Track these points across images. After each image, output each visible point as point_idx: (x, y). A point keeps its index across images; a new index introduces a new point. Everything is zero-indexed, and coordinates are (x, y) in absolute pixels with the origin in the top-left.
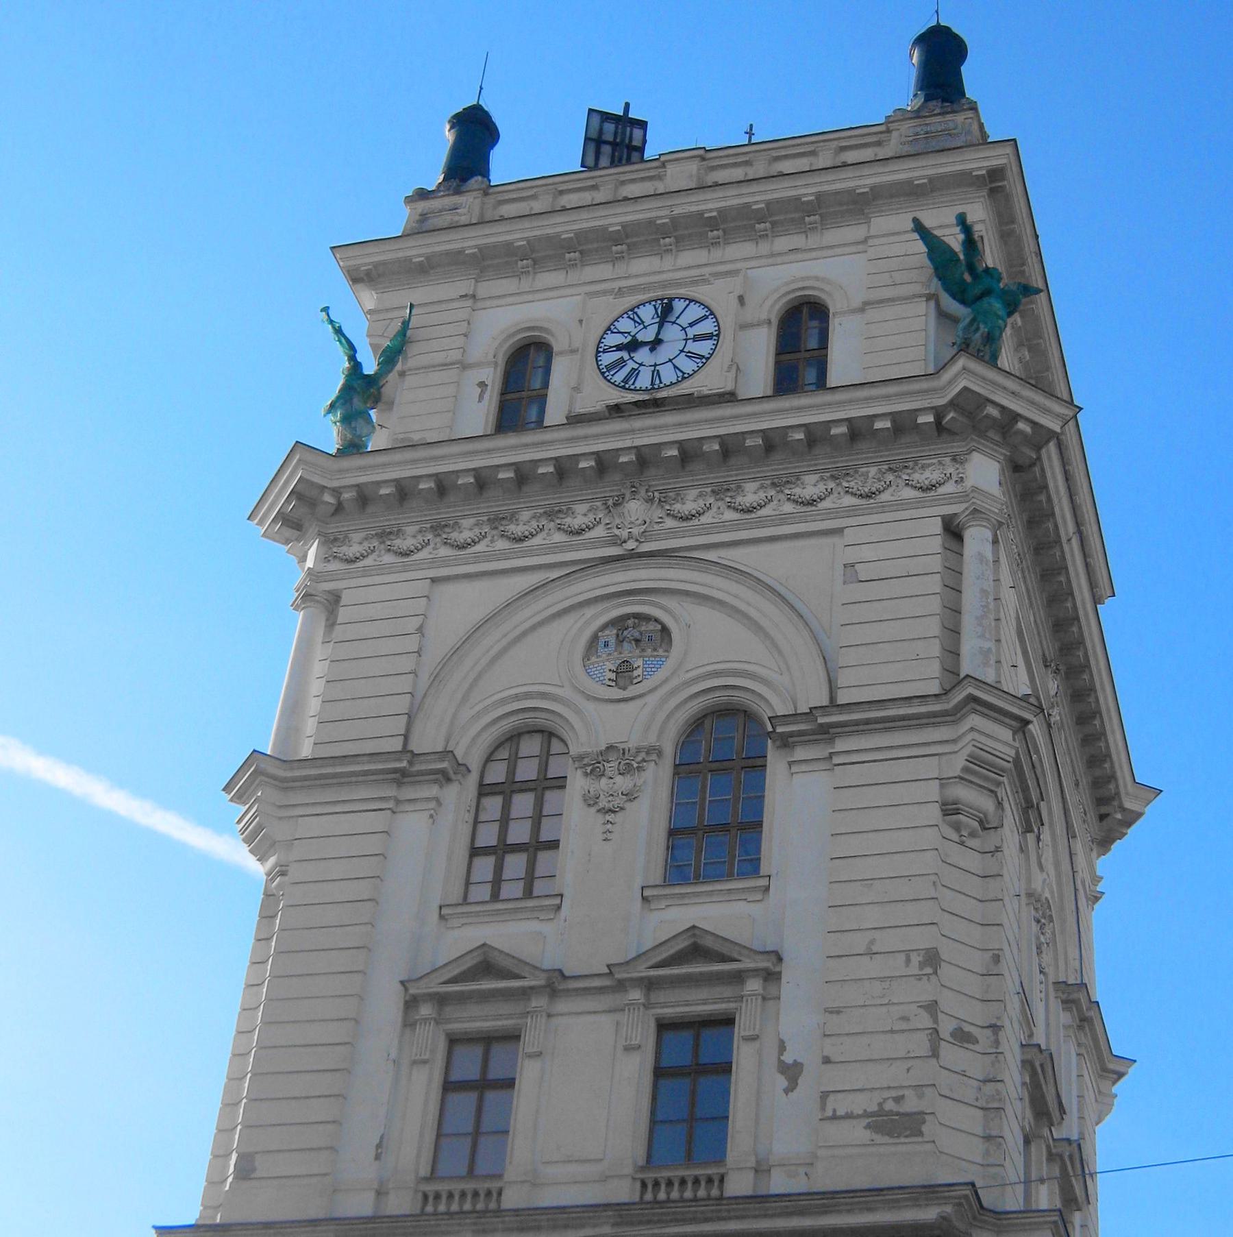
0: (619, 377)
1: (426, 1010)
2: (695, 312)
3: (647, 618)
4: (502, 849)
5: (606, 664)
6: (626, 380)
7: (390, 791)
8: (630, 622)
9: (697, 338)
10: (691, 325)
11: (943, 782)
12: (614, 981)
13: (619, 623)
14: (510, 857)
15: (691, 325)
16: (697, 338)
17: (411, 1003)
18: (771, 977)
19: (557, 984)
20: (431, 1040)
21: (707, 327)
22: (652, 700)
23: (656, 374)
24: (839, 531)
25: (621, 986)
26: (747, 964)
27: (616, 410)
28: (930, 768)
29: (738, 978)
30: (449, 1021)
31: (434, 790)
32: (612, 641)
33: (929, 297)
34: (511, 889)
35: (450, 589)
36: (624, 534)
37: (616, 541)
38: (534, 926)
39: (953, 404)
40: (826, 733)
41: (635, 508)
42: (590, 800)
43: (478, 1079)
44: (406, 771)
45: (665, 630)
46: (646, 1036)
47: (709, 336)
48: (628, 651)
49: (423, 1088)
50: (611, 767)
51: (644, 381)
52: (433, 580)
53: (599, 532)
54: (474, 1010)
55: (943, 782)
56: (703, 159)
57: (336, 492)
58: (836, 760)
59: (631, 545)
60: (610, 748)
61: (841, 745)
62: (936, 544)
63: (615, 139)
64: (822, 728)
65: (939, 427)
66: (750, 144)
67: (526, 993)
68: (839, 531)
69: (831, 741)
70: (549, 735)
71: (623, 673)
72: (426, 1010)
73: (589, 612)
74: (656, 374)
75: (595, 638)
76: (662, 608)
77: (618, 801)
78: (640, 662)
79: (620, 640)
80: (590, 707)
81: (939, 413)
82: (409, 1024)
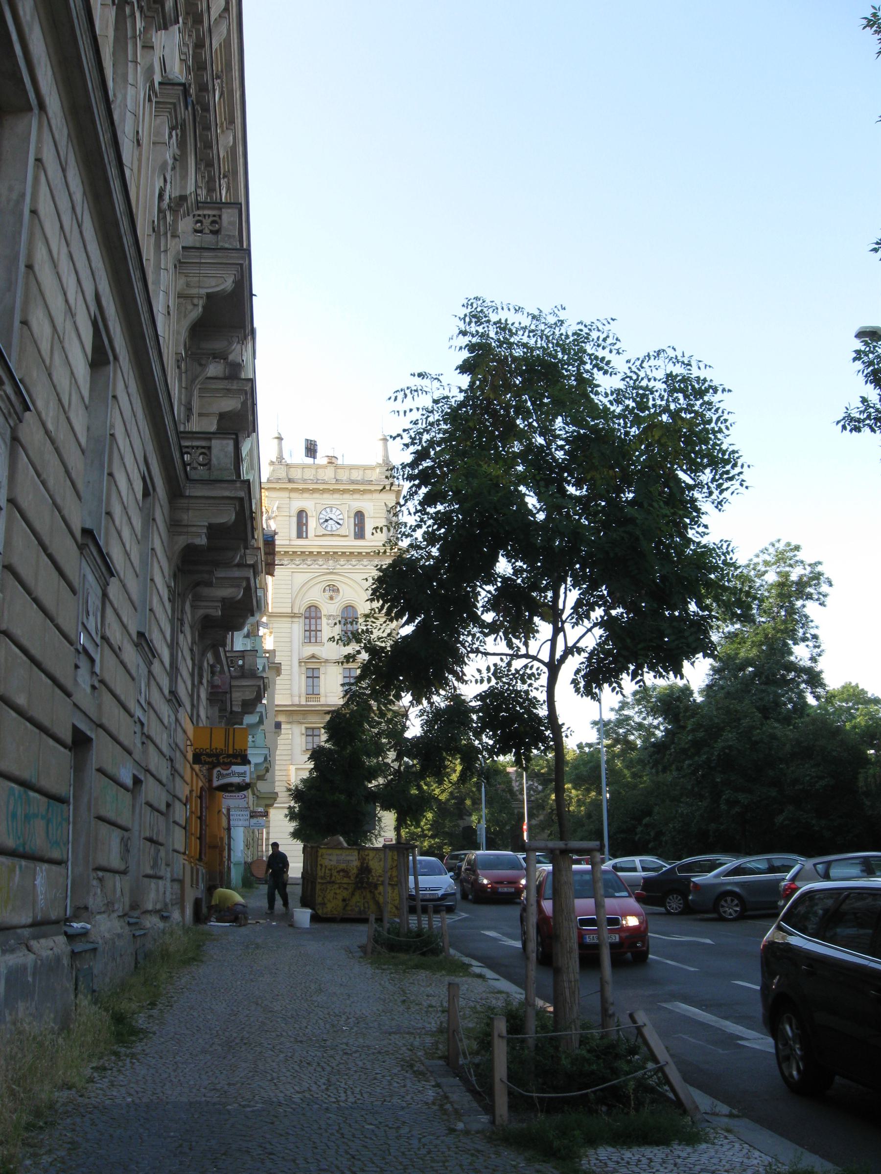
2: (338, 512)
4: (310, 631)
5: (328, 594)
14: (312, 634)
20: (304, 669)
21: (341, 517)
27: (324, 535)
34: (313, 640)
41: (331, 562)
44: (293, 616)
49: (303, 677)
51: (329, 528)
63: (311, 449)
70: (316, 607)
71: (331, 598)
82: (300, 666)
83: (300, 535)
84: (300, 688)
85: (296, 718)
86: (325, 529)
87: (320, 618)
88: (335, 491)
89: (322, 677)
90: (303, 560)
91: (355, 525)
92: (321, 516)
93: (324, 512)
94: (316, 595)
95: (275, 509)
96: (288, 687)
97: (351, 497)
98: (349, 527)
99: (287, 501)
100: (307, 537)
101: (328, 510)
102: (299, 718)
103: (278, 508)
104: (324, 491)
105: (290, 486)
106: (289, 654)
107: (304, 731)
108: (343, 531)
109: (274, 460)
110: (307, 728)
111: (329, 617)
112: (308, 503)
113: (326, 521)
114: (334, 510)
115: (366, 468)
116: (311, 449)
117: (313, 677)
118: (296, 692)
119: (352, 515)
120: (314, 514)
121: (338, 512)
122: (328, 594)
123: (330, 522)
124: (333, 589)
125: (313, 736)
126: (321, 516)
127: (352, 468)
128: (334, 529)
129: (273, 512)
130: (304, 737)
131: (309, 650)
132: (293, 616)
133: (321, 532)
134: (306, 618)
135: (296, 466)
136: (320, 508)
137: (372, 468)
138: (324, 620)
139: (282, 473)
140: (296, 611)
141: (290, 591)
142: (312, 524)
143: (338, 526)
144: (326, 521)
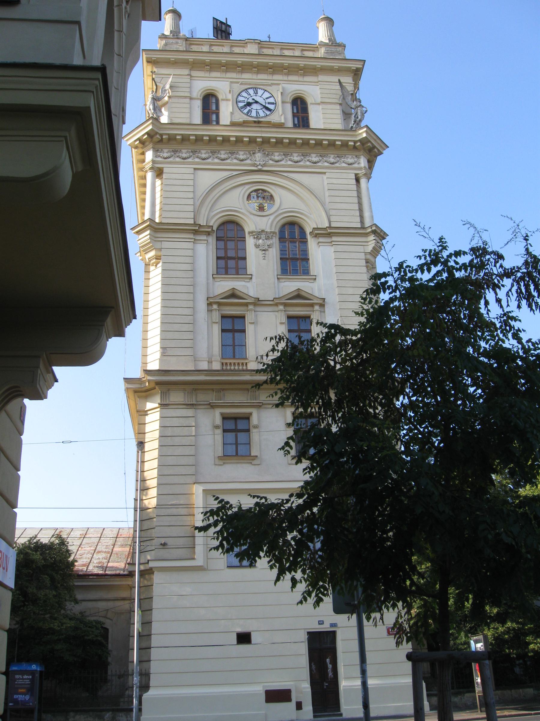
0: (246, 111)
1: (215, 307)
2: (267, 95)
3: (264, 191)
5: (254, 204)
6: (248, 112)
7: (192, 236)
8: (260, 191)
9: (269, 103)
10: (267, 98)
11: (366, 253)
12: (275, 303)
13: (256, 191)
15: (267, 98)
16: (269, 103)
17: (210, 304)
18: (322, 305)
19: (257, 302)
20: (216, 316)
21: (271, 100)
22: (272, 217)
23: (257, 113)
24: (325, 173)
25: (276, 305)
26: (315, 301)
28: (361, 249)
29: (312, 305)
30: (222, 310)
31: (204, 237)
32: (255, 197)
33: (340, 104)
35: (200, 173)
36: (258, 163)
37: (254, 165)
38: (243, 283)
39: (360, 141)
40: (329, 235)
41: (258, 156)
42: (257, 246)
43: (233, 328)
44: (196, 230)
45: (272, 196)
46: (284, 319)
47: (273, 104)
48: (261, 201)
49: (216, 329)
50: (263, 236)
51: (254, 114)
52: (195, 169)
53: (248, 162)
54: (228, 308)
55: (366, 253)
56: (259, 44)
57: (161, 135)
58: (333, 243)
59: (260, 167)
60: (263, 231)
61: (334, 239)
62: (354, 182)
63: (222, 30)
64: (327, 234)
65: (355, 147)
66: (270, 42)
67: (246, 305)
68: (325, 173)
69: (331, 237)
71: (261, 208)
72: (215, 307)
73: (247, 187)
74: (257, 113)
75: (249, 196)
76: (271, 189)
77: (266, 247)
78: (266, 205)
79: (258, 197)
80: (252, 217)
81: (355, 142)
82: (210, 311)
83: (206, 119)
84: (210, 347)
85: (202, 397)
86: (247, 114)
87: (243, 239)
88: (261, 68)
89: (250, 329)
90: (213, 152)
91: (294, 115)
92: (240, 98)
93: (244, 94)
94: (235, 202)
95: (167, 87)
96: (188, 343)
97: (285, 78)
98: (284, 114)
99: (187, 79)
100: (218, 122)
101: (251, 92)
102: (211, 397)
103: (171, 87)
104: (244, 68)
105: (191, 57)
106: (191, 289)
107: (218, 421)
108: (275, 118)
109: (167, 33)
110: (225, 418)
111: (257, 235)
112: (222, 85)
113: (249, 104)
114: (260, 92)
115: (305, 47)
116: (222, 30)
117: (233, 331)
118: (202, 352)
119: (289, 99)
120: (230, 96)
121: (267, 95)
122: (254, 204)
123: (255, 106)
124: (263, 196)
125: (236, 431)
126: (240, 98)
127: (284, 46)
128: (262, 114)
129: (164, 91)
130: (219, 431)
131: (224, 285)
132: (196, 230)
133: (240, 117)
134: (218, 239)
135: (201, 41)
136: (237, 88)
137: (315, 49)
138: (250, 242)
139: (181, 46)
140: (202, 222)
141: (191, 202)
142: (227, 112)
143: (268, 113)
144: (249, 104)
